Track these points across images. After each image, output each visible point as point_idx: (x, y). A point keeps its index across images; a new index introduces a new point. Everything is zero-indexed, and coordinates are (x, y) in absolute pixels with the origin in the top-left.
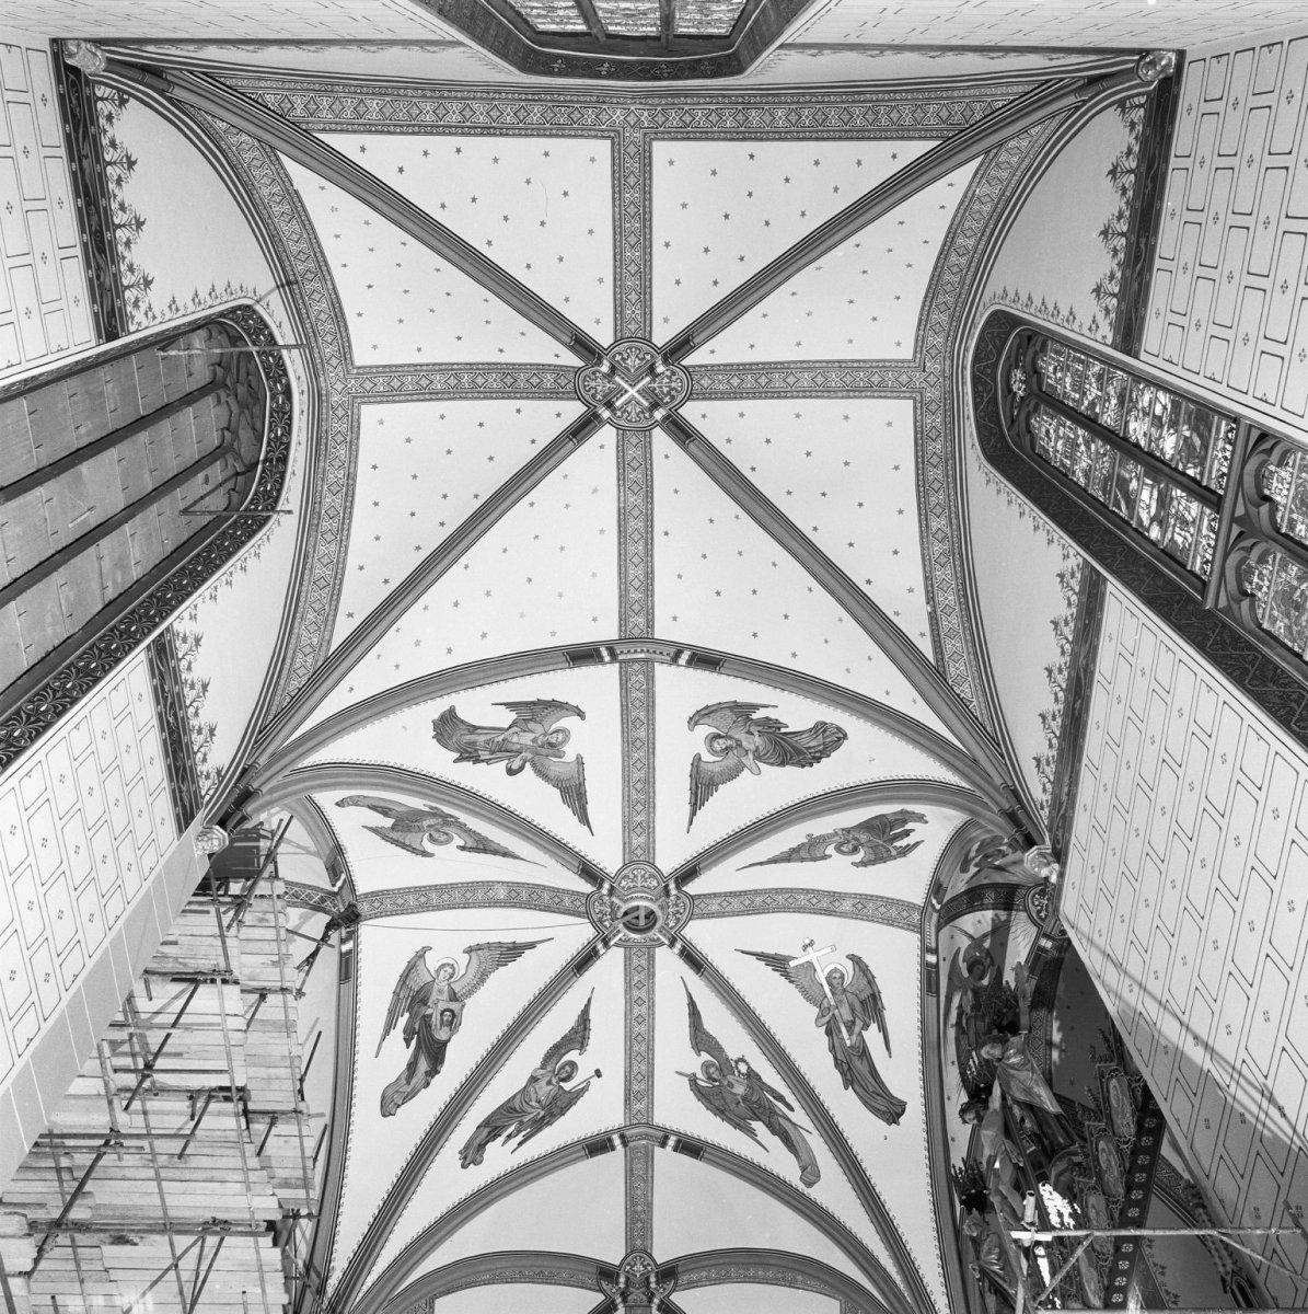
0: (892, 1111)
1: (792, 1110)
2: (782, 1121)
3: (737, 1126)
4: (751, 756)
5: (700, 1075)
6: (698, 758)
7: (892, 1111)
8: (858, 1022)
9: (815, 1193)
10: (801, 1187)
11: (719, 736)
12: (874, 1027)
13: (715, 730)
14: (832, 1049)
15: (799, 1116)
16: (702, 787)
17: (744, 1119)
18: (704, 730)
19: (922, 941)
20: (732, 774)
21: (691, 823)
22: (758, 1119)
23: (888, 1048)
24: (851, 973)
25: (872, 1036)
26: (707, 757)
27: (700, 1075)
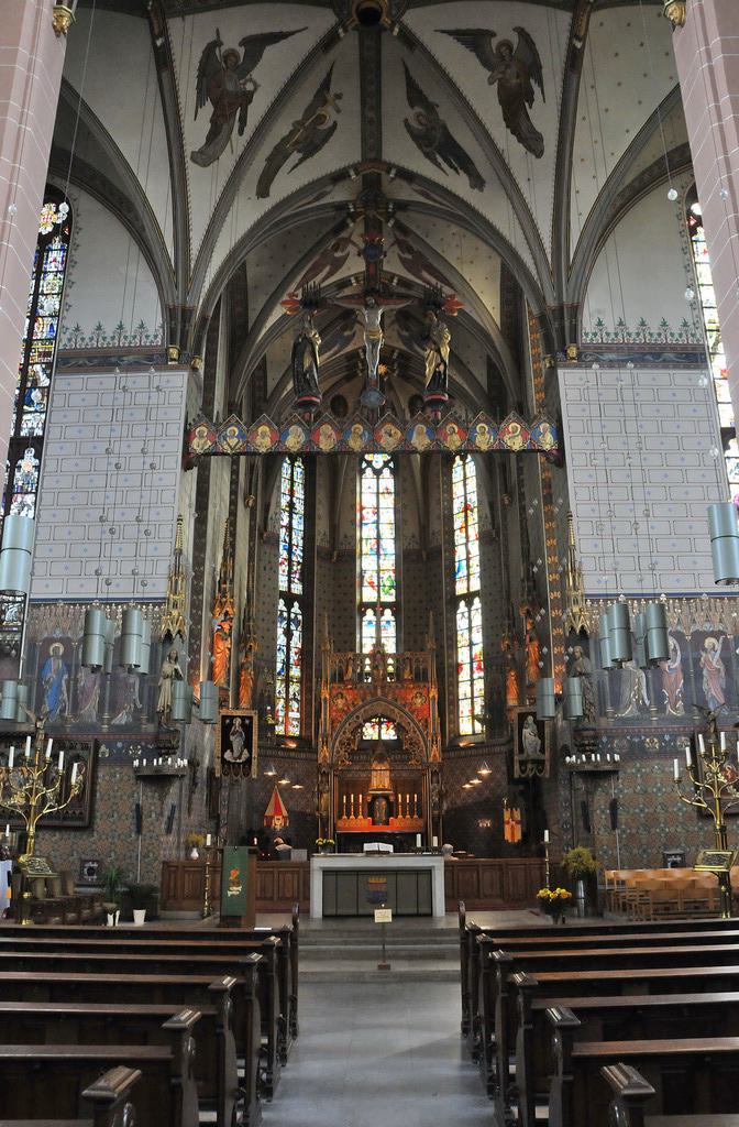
0: (263, 192)
1: (241, 132)
2: (225, 127)
3: (199, 88)
4: (500, 76)
5: (223, 49)
6: (493, 34)
7: (263, 192)
8: (301, 145)
9: (192, 169)
10: (188, 154)
11: (511, 50)
12: (300, 155)
13: (515, 46)
14: (283, 139)
15: (239, 142)
16: (474, 40)
17: (209, 95)
18: (515, 39)
19: (359, 163)
20: (486, 63)
21: (443, 32)
22: (215, 104)
23: (293, 169)
24: (326, 127)
25: (296, 156)
26: (495, 42)
27: (223, 49)
